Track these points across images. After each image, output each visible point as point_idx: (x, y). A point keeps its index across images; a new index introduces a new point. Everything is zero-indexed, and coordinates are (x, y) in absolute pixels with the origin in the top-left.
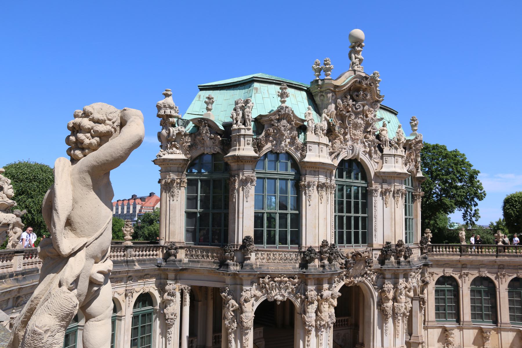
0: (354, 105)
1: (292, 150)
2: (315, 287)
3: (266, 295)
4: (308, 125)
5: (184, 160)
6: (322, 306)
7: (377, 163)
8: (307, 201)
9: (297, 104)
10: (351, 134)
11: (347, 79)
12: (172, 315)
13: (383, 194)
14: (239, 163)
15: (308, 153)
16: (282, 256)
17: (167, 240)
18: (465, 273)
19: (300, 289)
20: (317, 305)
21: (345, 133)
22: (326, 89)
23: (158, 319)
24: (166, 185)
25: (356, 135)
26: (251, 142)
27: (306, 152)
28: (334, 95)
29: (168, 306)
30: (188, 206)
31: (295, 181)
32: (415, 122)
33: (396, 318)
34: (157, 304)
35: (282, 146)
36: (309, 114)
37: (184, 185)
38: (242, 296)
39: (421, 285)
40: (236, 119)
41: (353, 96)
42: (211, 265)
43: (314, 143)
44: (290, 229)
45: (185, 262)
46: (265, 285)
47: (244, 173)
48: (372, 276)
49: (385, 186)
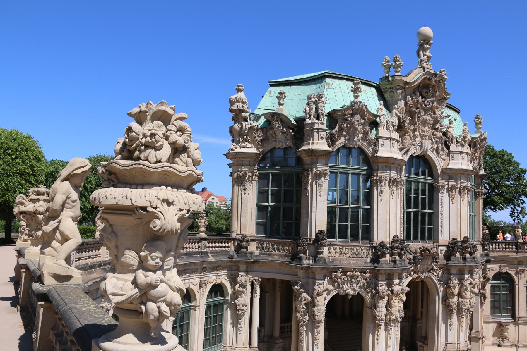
0: (424, 102)
1: (364, 145)
2: (386, 282)
3: (338, 289)
4: (380, 121)
5: (256, 153)
6: (392, 301)
7: (444, 160)
8: (379, 196)
9: (367, 99)
11: (416, 76)
12: (243, 306)
13: (450, 190)
14: (312, 158)
15: (381, 149)
17: (239, 233)
18: (521, 270)
19: (371, 284)
20: (387, 300)
22: (397, 85)
23: (229, 309)
24: (238, 179)
25: (425, 132)
26: (325, 137)
27: (379, 148)
28: (404, 91)
29: (240, 297)
30: (259, 200)
31: (366, 176)
32: (480, 120)
33: (460, 313)
34: (228, 295)
37: (255, 179)
38: (315, 289)
39: (482, 281)
40: (309, 113)
41: (423, 92)
42: (283, 258)
43: (386, 138)
44: (361, 224)
45: (256, 254)
46: (338, 279)
47: (318, 167)
48: (438, 272)
49: (452, 183)
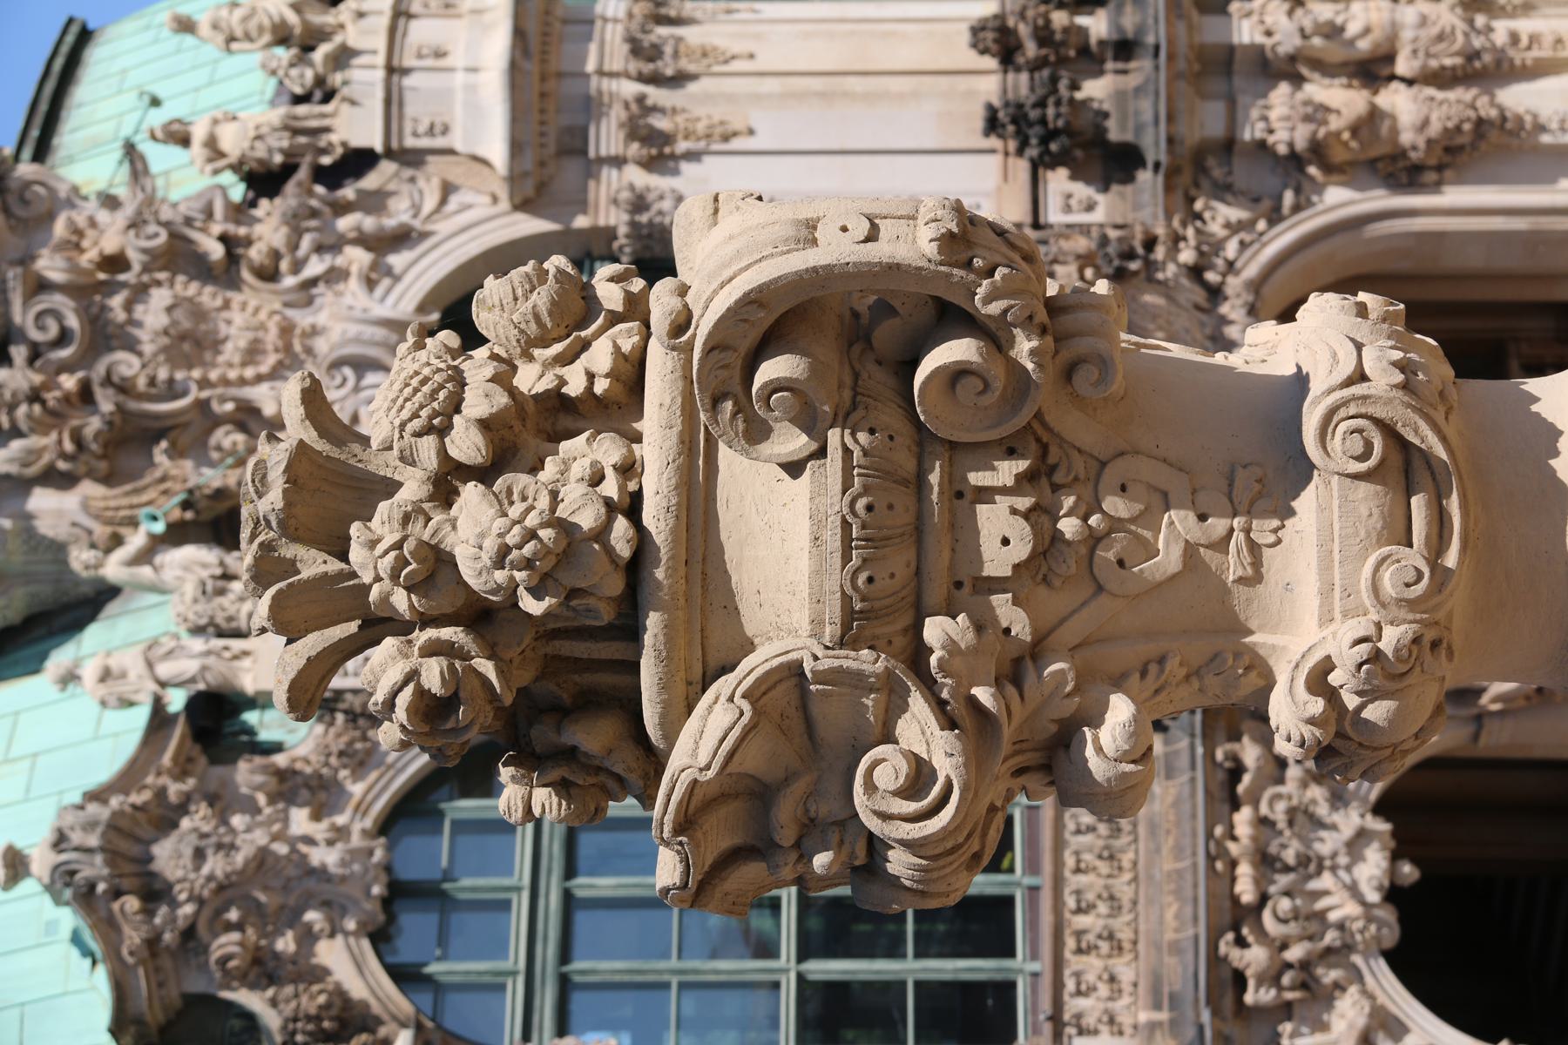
0: (36, 353)
3: (1357, 959)
4: (193, 680)
7: (447, 189)
10: (249, 372)
16: (1090, 850)
21: (240, 416)
25: (256, 341)
35: (343, 863)
36: (106, 675)
46: (1288, 966)
48: (1216, 228)
49: (608, 137)
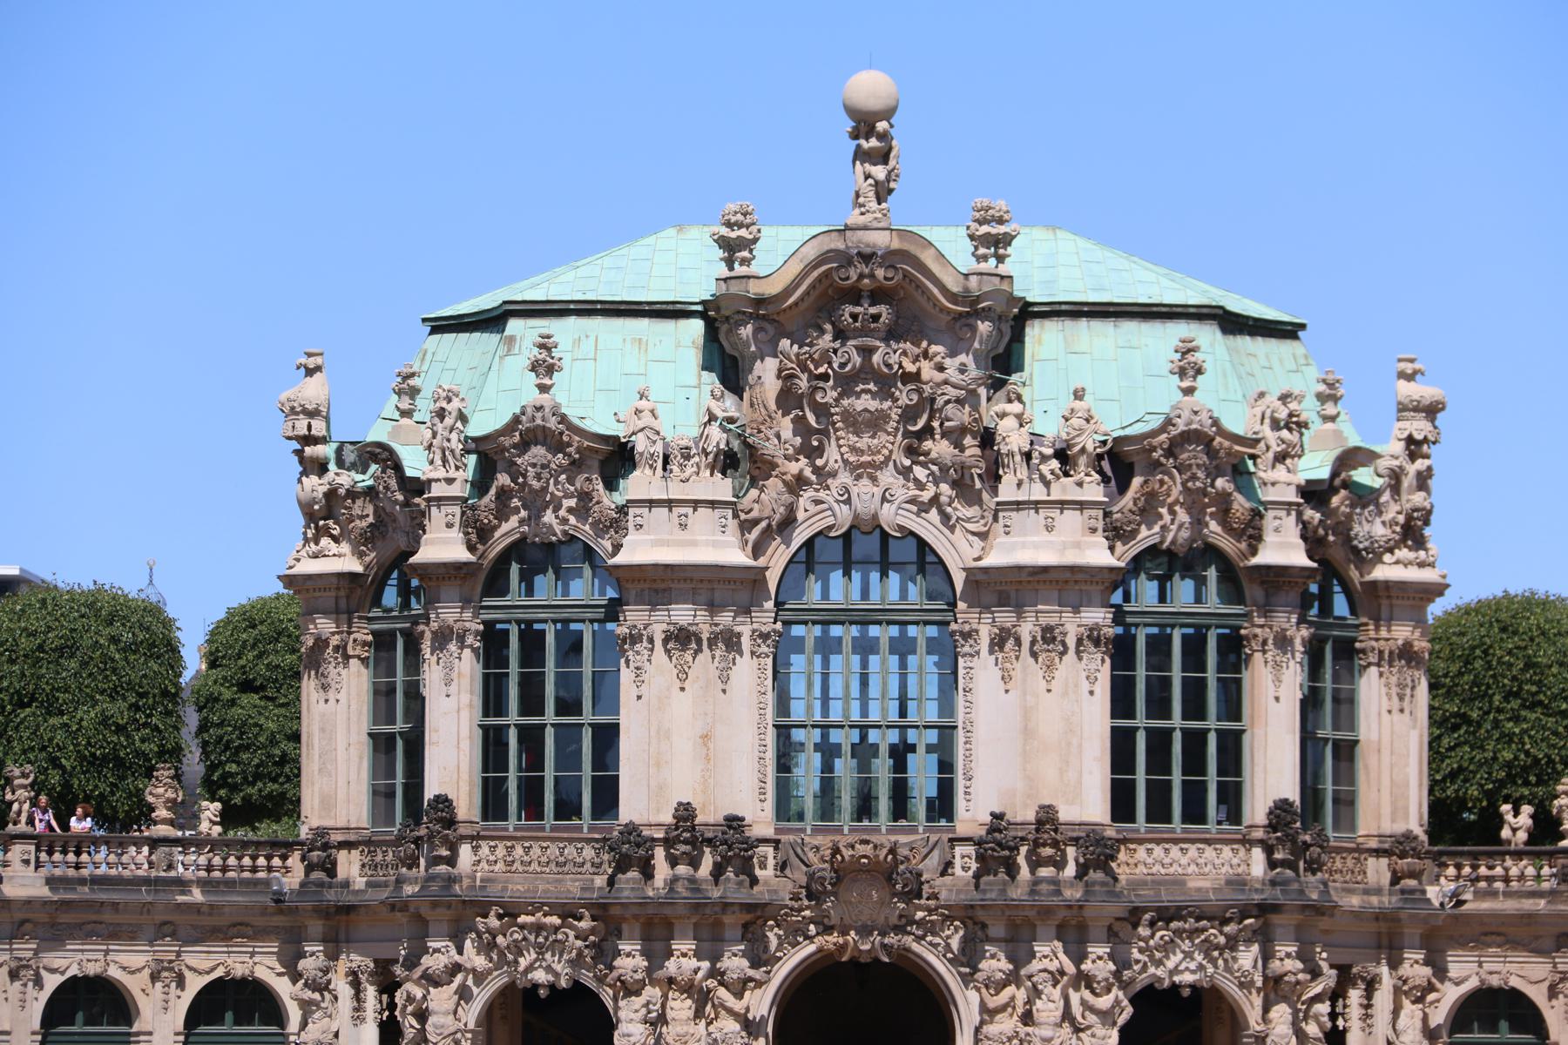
43: (651, 503)
49: (1005, 617)
